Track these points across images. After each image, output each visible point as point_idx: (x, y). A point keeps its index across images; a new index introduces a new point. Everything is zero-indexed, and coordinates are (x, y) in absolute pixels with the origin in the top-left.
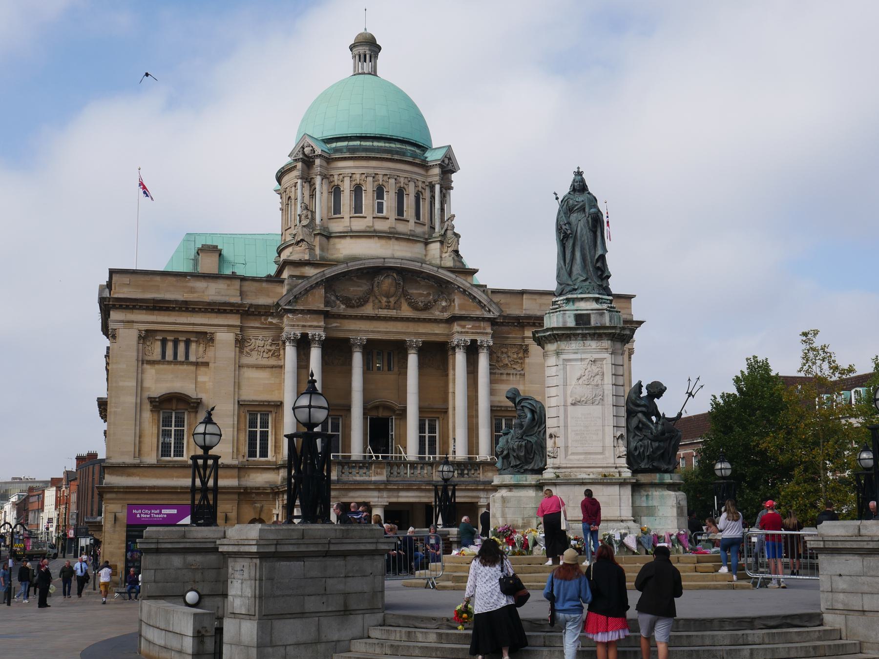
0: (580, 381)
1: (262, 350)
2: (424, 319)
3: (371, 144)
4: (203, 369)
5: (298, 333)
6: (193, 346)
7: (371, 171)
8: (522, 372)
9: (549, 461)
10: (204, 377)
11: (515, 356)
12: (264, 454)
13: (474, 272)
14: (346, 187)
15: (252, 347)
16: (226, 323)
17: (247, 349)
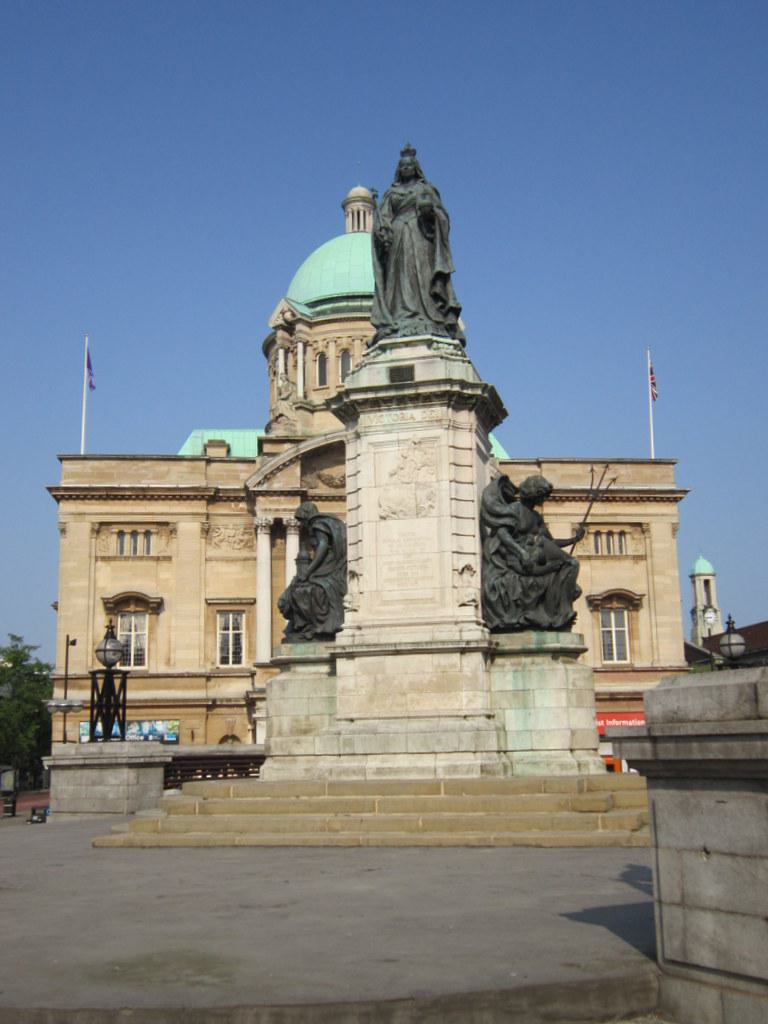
1: (234, 539)
4: (165, 564)
5: (271, 518)
6: (153, 539)
7: (358, 333)
9: (348, 616)
10: (165, 572)
12: (237, 660)
14: (332, 353)
15: (221, 537)
16: (190, 510)
17: (216, 540)
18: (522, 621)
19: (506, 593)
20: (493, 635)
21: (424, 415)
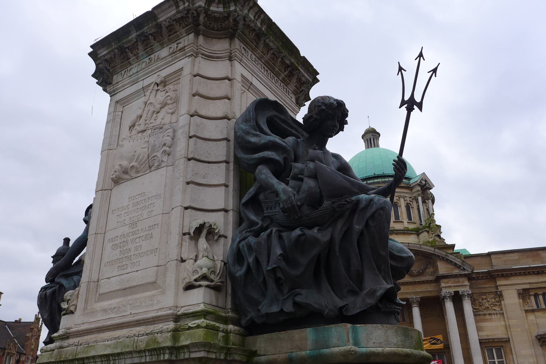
0: (134, 132)
2: (419, 282)
3: (373, 181)
8: (501, 312)
11: (493, 300)
13: (453, 246)
18: (289, 307)
19: (257, 261)
20: (250, 339)
21: (171, 50)
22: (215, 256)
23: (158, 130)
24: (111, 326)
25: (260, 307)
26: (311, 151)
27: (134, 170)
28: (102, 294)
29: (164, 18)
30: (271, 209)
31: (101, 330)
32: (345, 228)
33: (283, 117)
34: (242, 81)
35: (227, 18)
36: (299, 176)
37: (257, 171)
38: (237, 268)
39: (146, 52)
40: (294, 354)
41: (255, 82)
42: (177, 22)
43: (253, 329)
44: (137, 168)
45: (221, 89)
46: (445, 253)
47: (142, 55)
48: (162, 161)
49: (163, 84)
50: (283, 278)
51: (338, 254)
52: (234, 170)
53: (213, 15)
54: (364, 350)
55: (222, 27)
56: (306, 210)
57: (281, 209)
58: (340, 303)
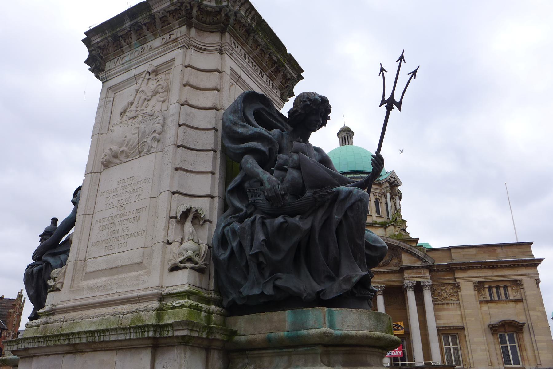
0: (125, 118)
8: (458, 302)
11: (451, 291)
13: (416, 240)
18: (269, 291)
19: (240, 245)
20: (231, 319)
21: (164, 41)
22: (200, 240)
23: (148, 117)
24: (97, 303)
25: (241, 290)
26: (296, 143)
27: (124, 155)
28: (89, 273)
29: (158, 9)
30: (255, 196)
31: (87, 308)
32: (325, 218)
33: (269, 110)
34: (231, 74)
35: (219, 12)
36: (284, 167)
37: (243, 160)
38: (222, 251)
39: (139, 42)
40: (272, 335)
41: (243, 76)
42: (170, 14)
43: (234, 309)
44: (126, 153)
45: (211, 80)
46: (409, 246)
47: (135, 44)
48: (152, 147)
49: (155, 73)
50: (265, 263)
51: (317, 241)
52: (221, 158)
53: (206, 9)
54: (339, 332)
55: (214, 21)
56: (289, 199)
57: (265, 197)
58: (318, 288)
